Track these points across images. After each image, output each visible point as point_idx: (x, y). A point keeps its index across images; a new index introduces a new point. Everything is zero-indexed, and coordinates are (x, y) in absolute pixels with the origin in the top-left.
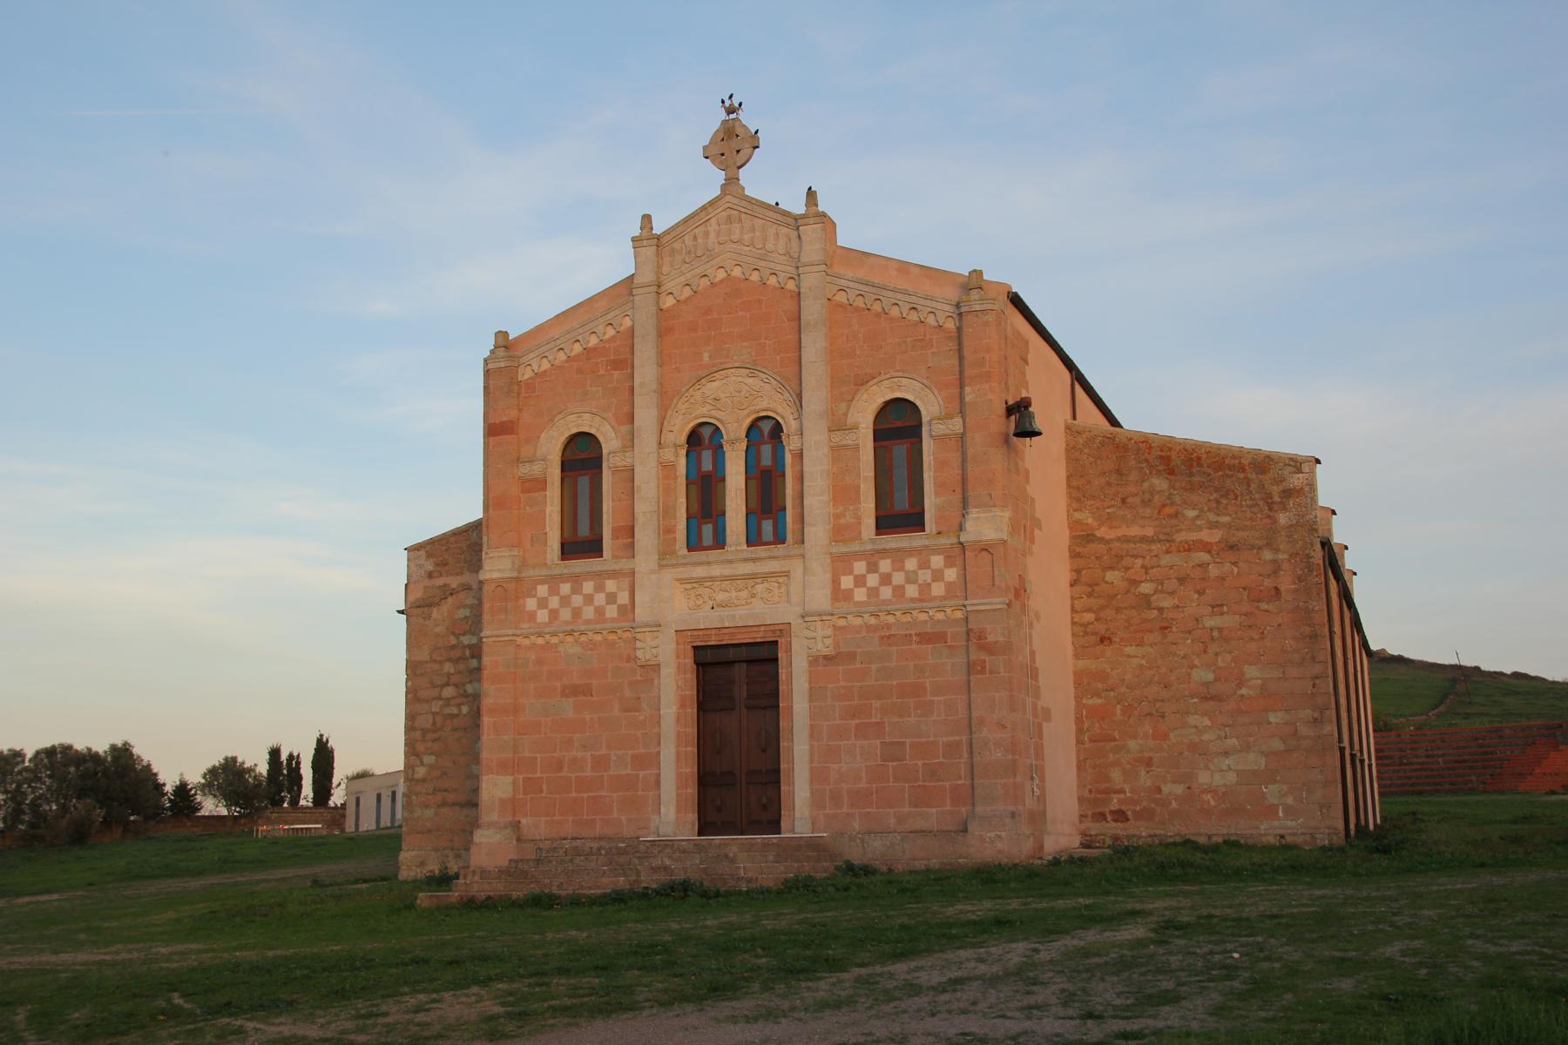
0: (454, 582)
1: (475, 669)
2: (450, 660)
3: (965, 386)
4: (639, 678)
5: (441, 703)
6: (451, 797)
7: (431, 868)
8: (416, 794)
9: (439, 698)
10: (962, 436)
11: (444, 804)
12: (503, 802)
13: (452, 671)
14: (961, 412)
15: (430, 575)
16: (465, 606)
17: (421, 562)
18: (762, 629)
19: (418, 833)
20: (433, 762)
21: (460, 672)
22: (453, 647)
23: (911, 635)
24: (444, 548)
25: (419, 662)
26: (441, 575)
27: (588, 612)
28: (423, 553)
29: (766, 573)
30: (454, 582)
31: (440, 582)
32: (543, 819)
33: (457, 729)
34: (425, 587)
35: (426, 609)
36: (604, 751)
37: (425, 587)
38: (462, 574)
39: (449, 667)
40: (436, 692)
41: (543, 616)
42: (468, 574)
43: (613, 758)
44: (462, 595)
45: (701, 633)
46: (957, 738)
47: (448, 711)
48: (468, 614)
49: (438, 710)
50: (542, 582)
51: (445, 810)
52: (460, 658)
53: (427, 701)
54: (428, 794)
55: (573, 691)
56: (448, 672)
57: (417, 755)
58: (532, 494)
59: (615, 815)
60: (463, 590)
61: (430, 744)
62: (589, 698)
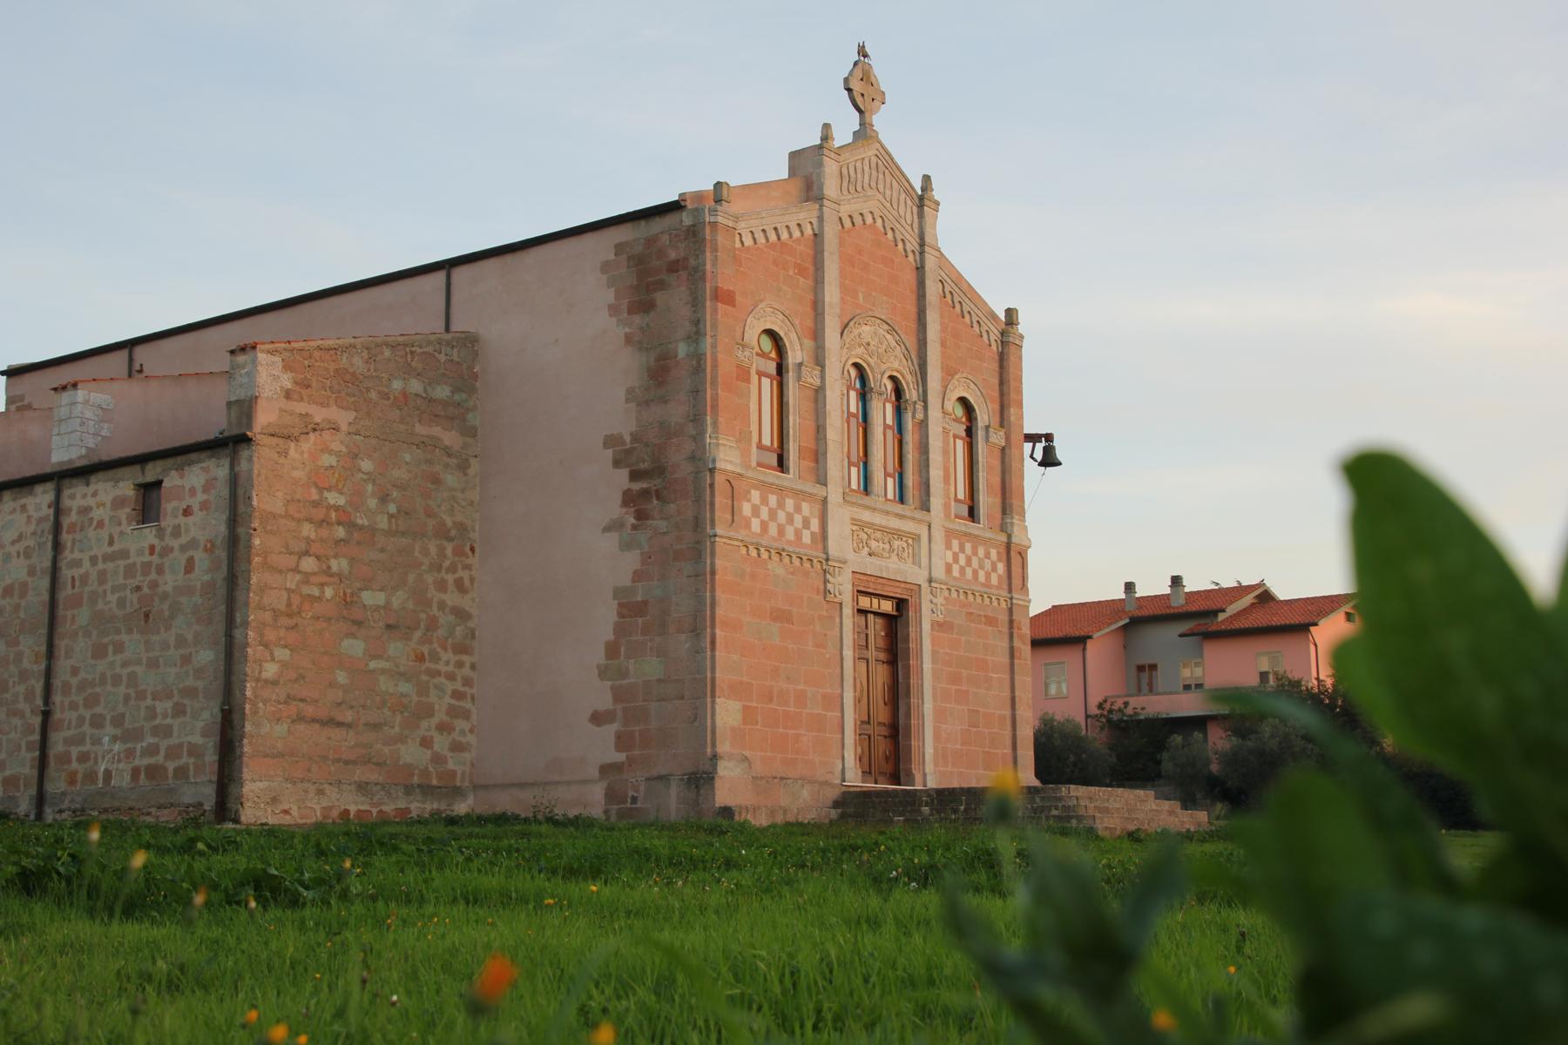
0: (319, 414)
1: (342, 540)
2: (310, 520)
3: (1009, 406)
4: (825, 613)
5: (298, 577)
6: (309, 710)
7: (286, 807)
8: (265, 702)
9: (296, 570)
10: (1003, 449)
11: (300, 718)
12: (733, 729)
13: (313, 536)
14: (1002, 425)
15: (288, 395)
16: (331, 452)
17: (276, 373)
18: (903, 585)
19: (266, 756)
20: (288, 658)
21: (322, 540)
22: (316, 504)
23: (980, 615)
24: (306, 363)
25: (271, 513)
26: (302, 400)
27: (790, 534)
28: (278, 359)
29: (904, 532)
30: (319, 414)
31: (301, 408)
32: (759, 754)
33: (318, 618)
34: (281, 410)
35: (281, 441)
36: (801, 687)
37: (281, 410)
38: (328, 406)
39: (307, 530)
40: (291, 561)
41: (756, 525)
42: (335, 407)
43: (809, 695)
44: (327, 435)
45: (865, 578)
46: (1004, 712)
47: (306, 590)
48: (334, 464)
49: (294, 587)
50: (756, 488)
51: (301, 727)
52: (323, 521)
53: (281, 571)
54: (279, 703)
55: (780, 616)
56: (308, 537)
57: (266, 646)
58: (739, 383)
59: (811, 757)
60: (329, 429)
61: (282, 632)
62: (791, 626)
